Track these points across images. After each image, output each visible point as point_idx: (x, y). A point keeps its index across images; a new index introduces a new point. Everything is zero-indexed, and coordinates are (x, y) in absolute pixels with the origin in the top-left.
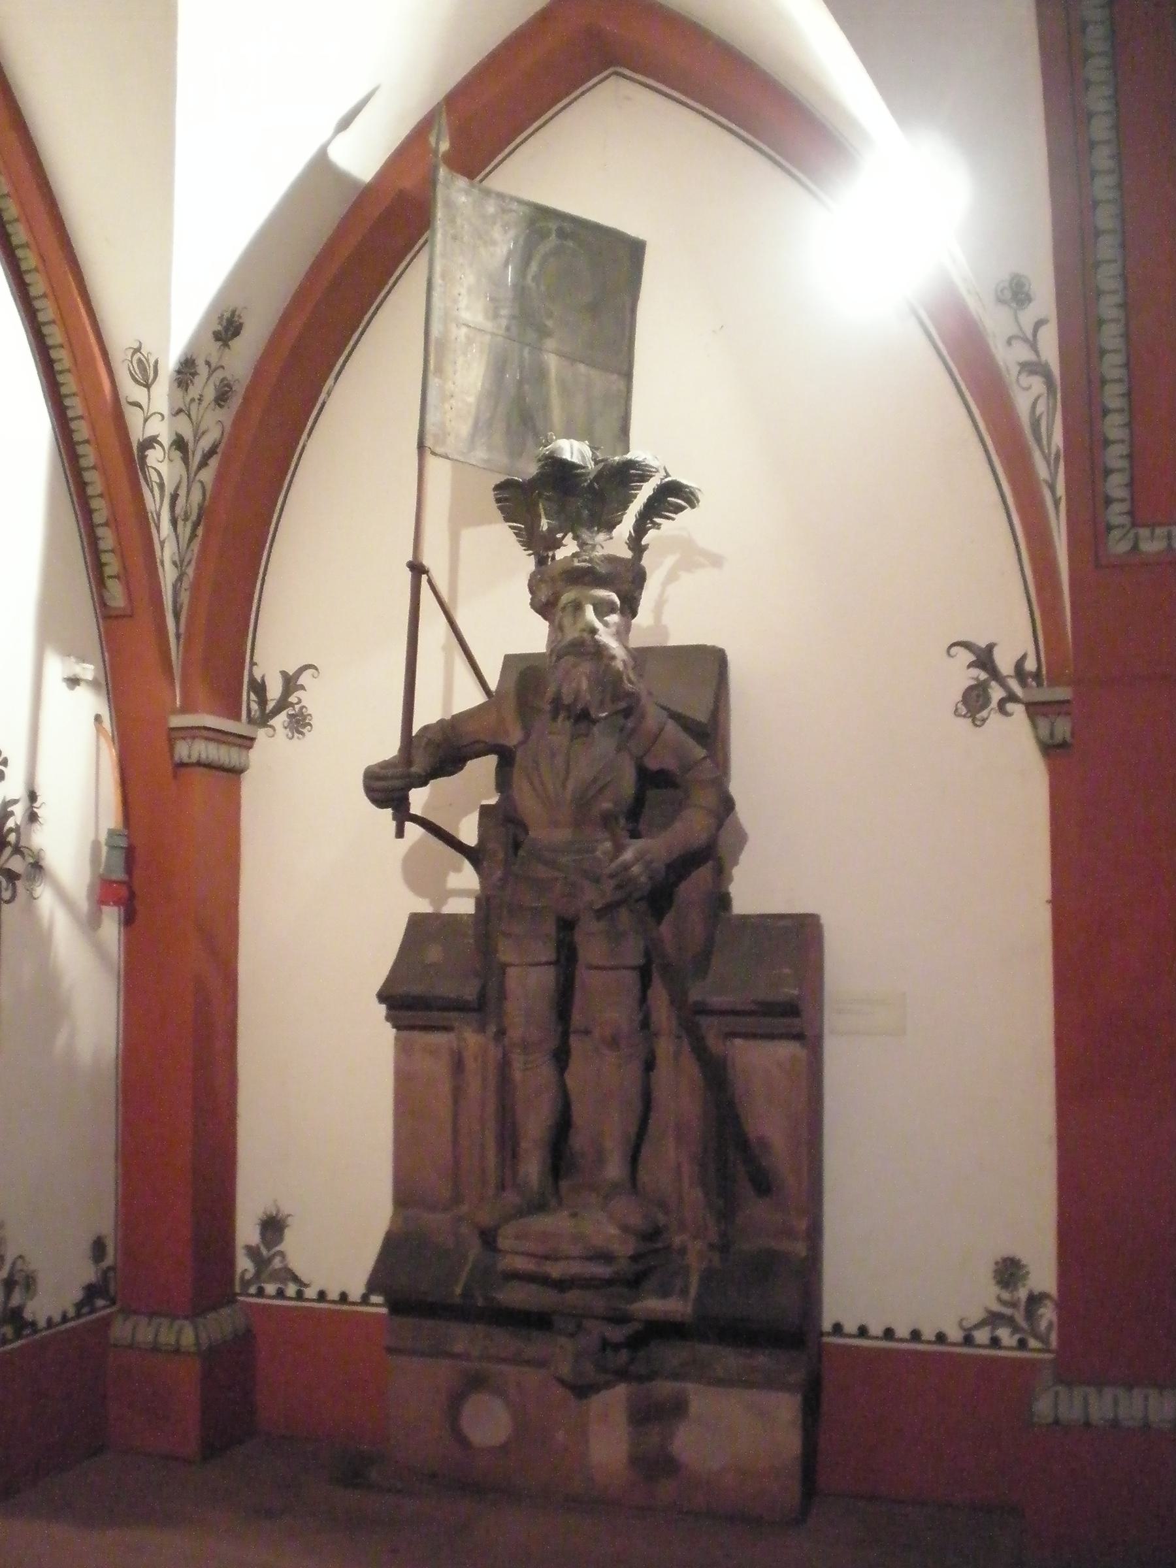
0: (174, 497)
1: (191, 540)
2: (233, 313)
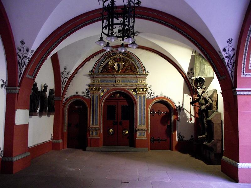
0: (191, 82)
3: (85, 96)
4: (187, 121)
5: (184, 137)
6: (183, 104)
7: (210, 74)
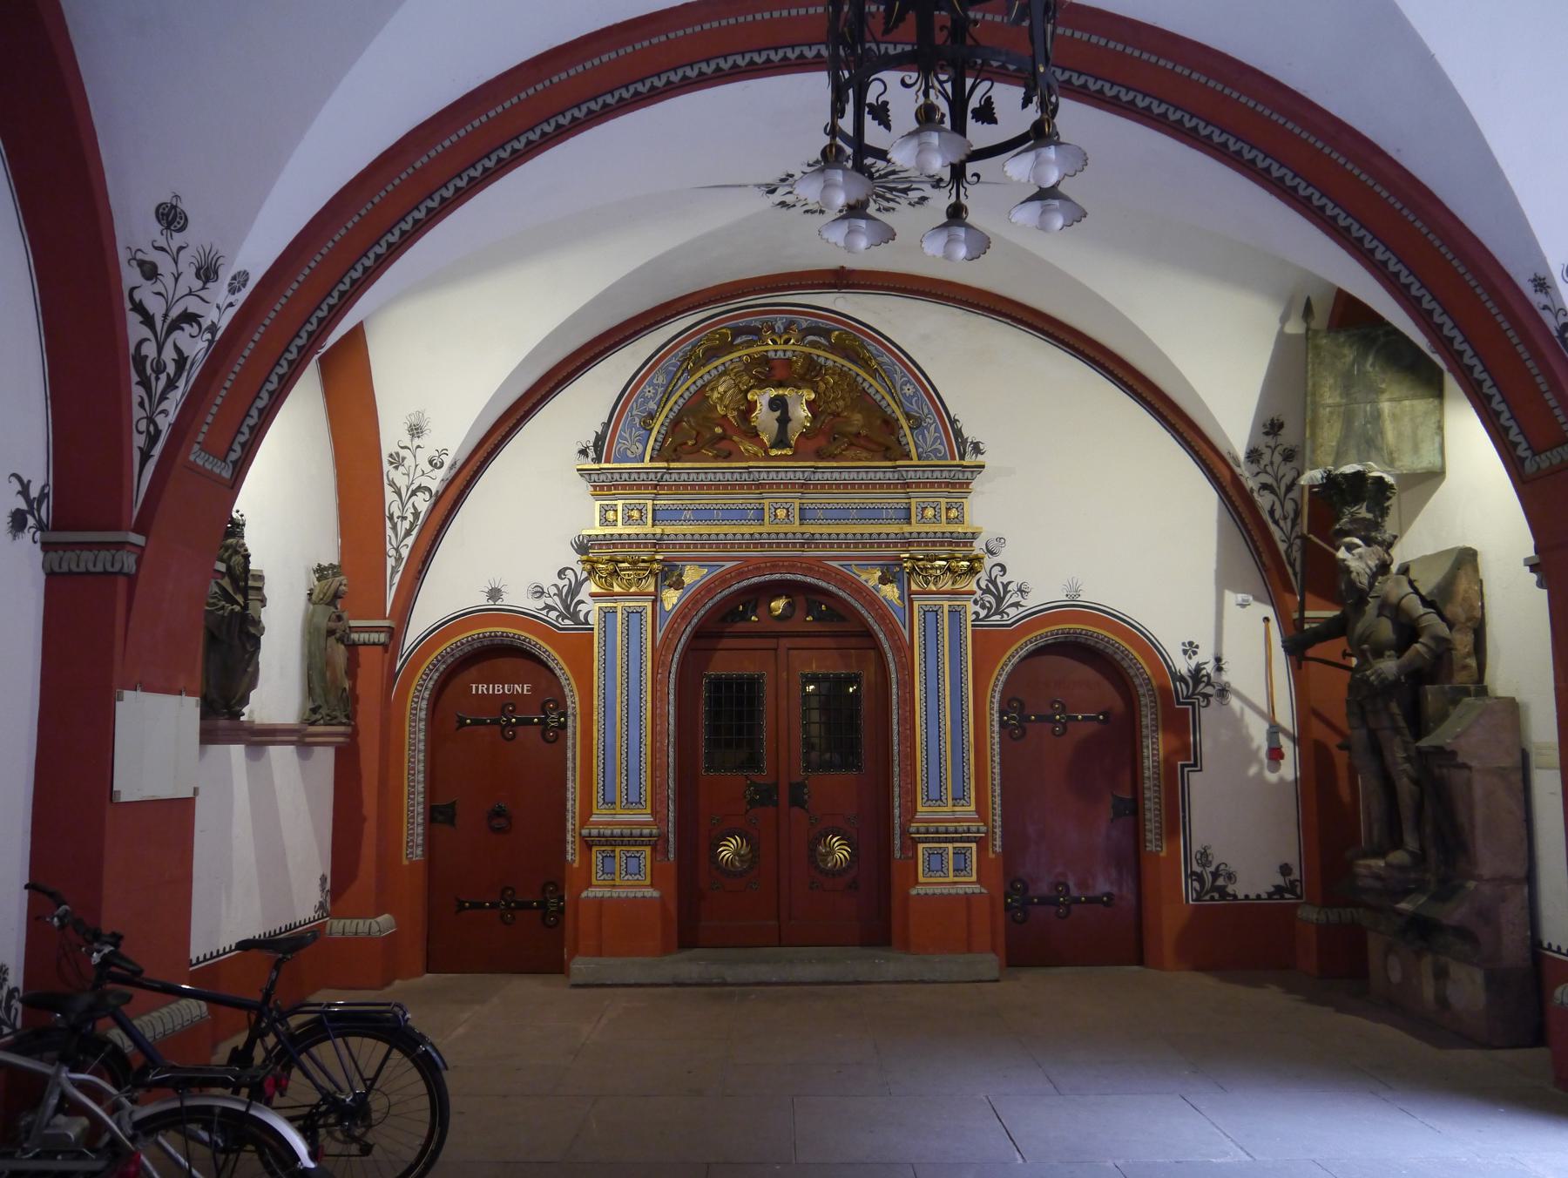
0: (1272, 512)
3: (553, 614)
4: (1253, 770)
5: (1230, 877)
6: (1218, 660)
7: (1416, 449)
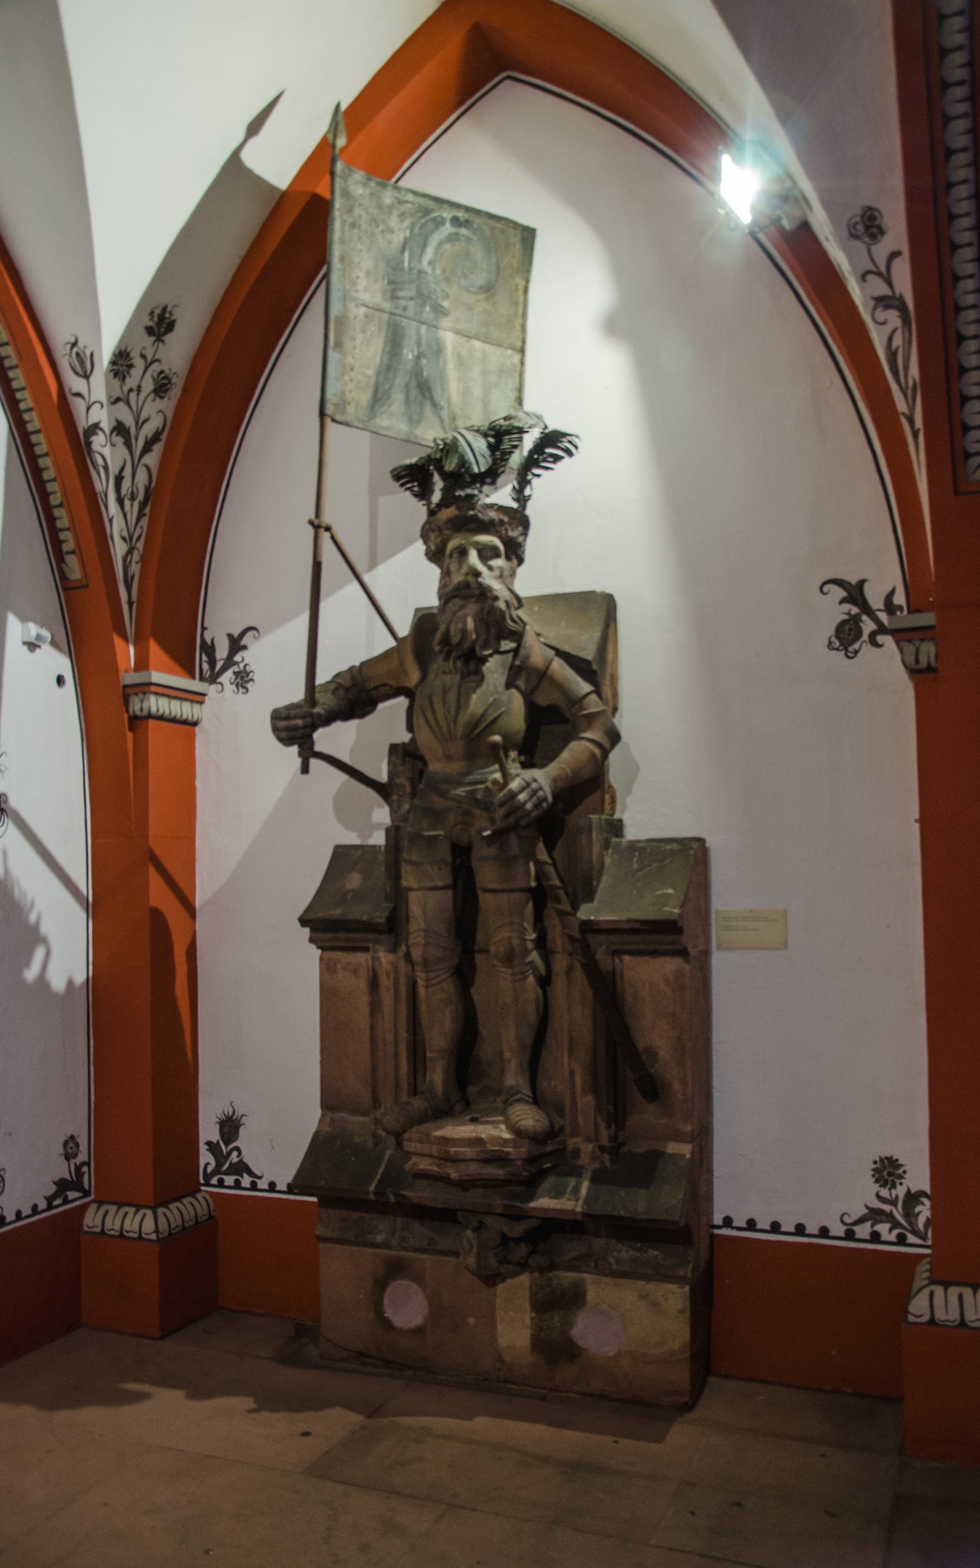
0: (119, 479)
1: (139, 519)
2: (164, 309)
